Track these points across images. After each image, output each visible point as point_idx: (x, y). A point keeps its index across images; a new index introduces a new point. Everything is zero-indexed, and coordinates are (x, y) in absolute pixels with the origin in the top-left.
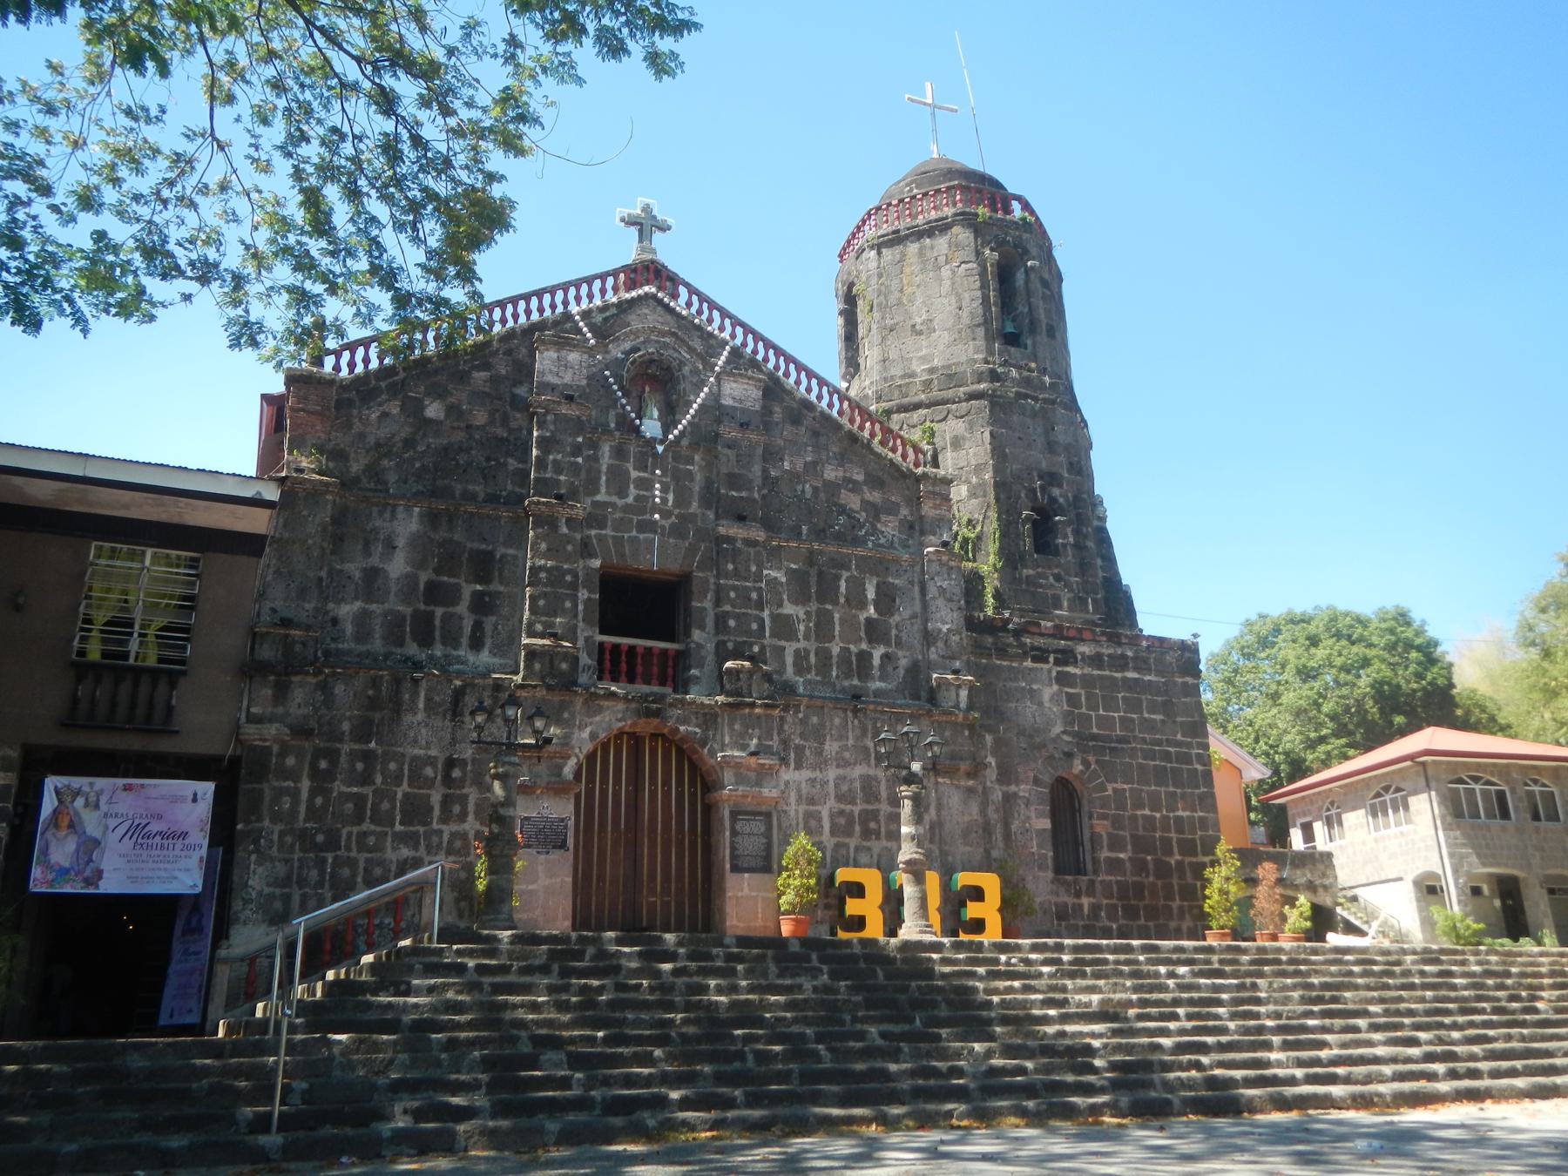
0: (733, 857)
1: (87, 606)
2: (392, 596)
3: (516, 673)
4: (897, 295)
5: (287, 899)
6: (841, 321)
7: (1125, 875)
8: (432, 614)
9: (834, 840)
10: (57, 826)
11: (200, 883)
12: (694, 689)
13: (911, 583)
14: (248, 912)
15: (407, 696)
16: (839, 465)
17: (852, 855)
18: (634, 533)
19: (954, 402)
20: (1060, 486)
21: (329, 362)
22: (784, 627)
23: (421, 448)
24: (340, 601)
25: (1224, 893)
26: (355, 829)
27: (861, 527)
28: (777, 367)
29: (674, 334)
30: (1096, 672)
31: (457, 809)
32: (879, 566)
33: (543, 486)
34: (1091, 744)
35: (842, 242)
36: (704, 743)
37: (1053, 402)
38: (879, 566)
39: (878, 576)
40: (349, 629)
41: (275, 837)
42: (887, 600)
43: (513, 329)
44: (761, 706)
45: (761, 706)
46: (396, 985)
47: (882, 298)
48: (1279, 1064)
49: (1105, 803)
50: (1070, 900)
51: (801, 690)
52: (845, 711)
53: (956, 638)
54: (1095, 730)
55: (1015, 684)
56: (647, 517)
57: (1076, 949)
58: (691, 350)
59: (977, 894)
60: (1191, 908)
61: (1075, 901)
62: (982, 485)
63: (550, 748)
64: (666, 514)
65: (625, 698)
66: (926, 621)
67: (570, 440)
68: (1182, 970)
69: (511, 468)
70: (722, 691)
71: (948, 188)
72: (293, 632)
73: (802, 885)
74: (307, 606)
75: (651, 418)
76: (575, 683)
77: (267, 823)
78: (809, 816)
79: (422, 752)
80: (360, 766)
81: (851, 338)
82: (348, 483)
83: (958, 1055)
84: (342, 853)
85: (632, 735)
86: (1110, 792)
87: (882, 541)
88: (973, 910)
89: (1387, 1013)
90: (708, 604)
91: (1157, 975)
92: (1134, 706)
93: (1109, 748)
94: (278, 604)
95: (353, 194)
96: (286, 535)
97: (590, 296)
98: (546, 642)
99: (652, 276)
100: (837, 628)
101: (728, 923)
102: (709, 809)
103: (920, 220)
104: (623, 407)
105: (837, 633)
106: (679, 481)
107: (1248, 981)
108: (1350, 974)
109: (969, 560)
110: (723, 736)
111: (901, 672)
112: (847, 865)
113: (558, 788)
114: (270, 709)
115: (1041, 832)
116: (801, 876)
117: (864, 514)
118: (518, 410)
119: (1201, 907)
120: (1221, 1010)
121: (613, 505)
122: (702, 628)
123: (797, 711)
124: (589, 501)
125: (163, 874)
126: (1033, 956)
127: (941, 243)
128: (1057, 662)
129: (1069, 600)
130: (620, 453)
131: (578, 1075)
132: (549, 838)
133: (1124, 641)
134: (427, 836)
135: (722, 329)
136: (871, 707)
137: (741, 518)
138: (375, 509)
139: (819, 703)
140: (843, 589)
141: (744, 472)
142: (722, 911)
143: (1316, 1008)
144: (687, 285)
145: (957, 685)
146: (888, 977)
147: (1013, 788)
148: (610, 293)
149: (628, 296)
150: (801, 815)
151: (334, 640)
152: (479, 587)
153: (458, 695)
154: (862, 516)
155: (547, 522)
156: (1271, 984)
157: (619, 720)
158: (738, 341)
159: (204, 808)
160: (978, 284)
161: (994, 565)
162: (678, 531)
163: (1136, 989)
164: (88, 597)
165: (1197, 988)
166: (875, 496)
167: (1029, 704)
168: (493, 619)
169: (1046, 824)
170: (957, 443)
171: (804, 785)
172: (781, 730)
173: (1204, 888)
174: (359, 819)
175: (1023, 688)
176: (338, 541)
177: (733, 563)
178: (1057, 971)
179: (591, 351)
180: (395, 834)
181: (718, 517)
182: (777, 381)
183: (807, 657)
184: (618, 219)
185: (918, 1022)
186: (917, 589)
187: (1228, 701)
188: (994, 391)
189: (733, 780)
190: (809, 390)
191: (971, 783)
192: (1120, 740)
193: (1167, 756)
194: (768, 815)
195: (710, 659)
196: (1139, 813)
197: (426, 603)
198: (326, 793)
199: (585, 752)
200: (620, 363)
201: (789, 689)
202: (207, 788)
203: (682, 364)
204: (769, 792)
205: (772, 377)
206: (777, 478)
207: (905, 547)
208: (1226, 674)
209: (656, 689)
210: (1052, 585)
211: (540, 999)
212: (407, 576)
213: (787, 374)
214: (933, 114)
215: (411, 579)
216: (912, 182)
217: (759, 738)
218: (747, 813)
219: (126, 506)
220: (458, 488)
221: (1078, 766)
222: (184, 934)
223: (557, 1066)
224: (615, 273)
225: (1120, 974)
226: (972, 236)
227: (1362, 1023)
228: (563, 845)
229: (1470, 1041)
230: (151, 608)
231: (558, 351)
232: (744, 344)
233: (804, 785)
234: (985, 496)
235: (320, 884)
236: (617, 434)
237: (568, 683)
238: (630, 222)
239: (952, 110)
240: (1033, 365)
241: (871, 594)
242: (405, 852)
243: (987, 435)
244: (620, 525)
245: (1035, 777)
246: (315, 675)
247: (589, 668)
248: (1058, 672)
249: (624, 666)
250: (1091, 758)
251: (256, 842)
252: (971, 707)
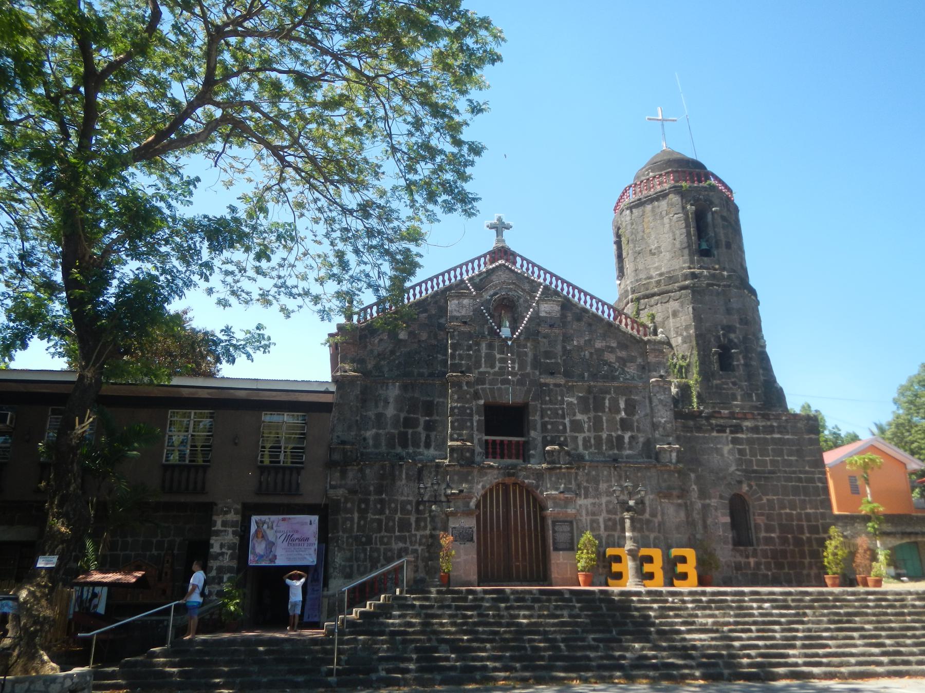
0: (554, 543)
1: (263, 440)
2: (389, 426)
3: (446, 458)
4: (641, 234)
5: (351, 567)
6: (615, 247)
7: (775, 545)
8: (407, 432)
9: (607, 533)
10: (257, 537)
11: (315, 560)
12: (532, 461)
13: (644, 398)
14: (335, 573)
15: (397, 473)
16: (603, 340)
17: (616, 541)
18: (499, 385)
19: (672, 292)
20: (735, 332)
21: (355, 318)
22: (577, 426)
23: (398, 354)
24: (367, 429)
25: (835, 554)
26: (378, 535)
27: (616, 372)
28: (568, 293)
29: (514, 284)
30: (755, 436)
31: (422, 524)
32: (626, 391)
33: (455, 367)
34: (753, 475)
35: (614, 205)
36: (537, 487)
37: (729, 286)
38: (626, 391)
39: (625, 395)
40: (371, 442)
41: (345, 540)
42: (631, 407)
43: (437, 291)
44: (565, 468)
45: (565, 468)
46: (386, 614)
47: (634, 236)
48: (794, 656)
49: (762, 507)
50: (743, 560)
51: (587, 457)
52: (610, 467)
53: (669, 425)
54: (755, 468)
55: (706, 446)
56: (505, 377)
57: (714, 594)
58: (523, 290)
59: (683, 560)
61: (746, 560)
62: (689, 336)
63: (464, 494)
64: (513, 374)
65: (498, 468)
66: (652, 417)
67: (466, 343)
68: (767, 605)
69: (439, 359)
70: (545, 461)
71: (666, 173)
72: (346, 447)
73: (588, 558)
74: (352, 433)
75: (505, 327)
76: (473, 462)
77: (341, 533)
78: (592, 521)
79: (405, 498)
80: (379, 506)
81: (620, 257)
82: (366, 374)
83: (627, 649)
84: (373, 546)
85: (503, 484)
86: (765, 501)
87: (628, 377)
88: (681, 568)
89: (876, 629)
90: (537, 418)
91: (752, 608)
92: (780, 453)
93: (764, 477)
94: (340, 434)
95: (357, 251)
96: (341, 402)
97: (473, 269)
98: (459, 443)
99: (503, 254)
100: (605, 425)
101: (553, 576)
102: (543, 519)
103: (652, 192)
104: (491, 323)
105: (605, 427)
106: (520, 358)
107: (801, 611)
108: (868, 607)
109: (682, 378)
111: (640, 445)
112: (614, 546)
113: (468, 513)
114: (339, 482)
115: (724, 524)
116: (588, 553)
117: (617, 364)
119: (823, 562)
120: (777, 627)
121: (489, 373)
122: (535, 430)
123: (584, 468)
124: (476, 372)
125: (300, 556)
126: (686, 598)
127: (664, 204)
128: (732, 432)
129: (741, 395)
130: (490, 346)
131: (453, 656)
132: (463, 537)
133: (772, 417)
134: (410, 538)
135: (539, 276)
136: (623, 464)
137: (552, 374)
138: (379, 386)
139: (596, 464)
140: (607, 404)
141: (552, 349)
142: (550, 569)
143: (832, 626)
144: (521, 256)
145: (670, 449)
146: (608, 610)
147: (708, 501)
148: (483, 266)
149: (491, 267)
150: (588, 522)
151: (365, 448)
152: (427, 418)
153: (420, 471)
154: (617, 365)
155: (457, 385)
156: (814, 613)
157: (495, 479)
158: (548, 282)
159: (315, 528)
160: (684, 225)
161: (696, 380)
162: (521, 383)
163: (736, 616)
164: (263, 437)
165: (771, 615)
166: (623, 354)
167: (715, 455)
168: (435, 433)
169: (728, 519)
170: (675, 314)
171: (589, 506)
172: (576, 479)
173: (823, 551)
174: (380, 531)
175: (712, 448)
176: (364, 401)
178: (696, 606)
179: (474, 298)
180: (396, 537)
181: (540, 374)
182: (568, 300)
183: (589, 441)
184: (485, 227)
185: (614, 633)
186: (647, 401)
187: (911, 414)
188: (694, 284)
189: (552, 505)
190: (585, 302)
191: (680, 501)
192: (771, 472)
193: (800, 480)
194: (571, 523)
195: (540, 445)
196: (782, 511)
197: (404, 427)
198: (365, 519)
200: (488, 301)
201: (581, 458)
202: (315, 518)
203: (519, 297)
204: (571, 511)
205: (566, 299)
206: (570, 350)
207: (641, 378)
208: (910, 398)
209: (514, 461)
210: (731, 388)
211: (444, 621)
212: (395, 415)
213: (574, 296)
214: (663, 125)
215: (396, 418)
216: (649, 168)
217: (565, 484)
218: (560, 522)
219: (275, 396)
220: (416, 371)
221: (745, 488)
222: (312, 581)
223: (446, 651)
224: (485, 256)
225: (731, 608)
226: (680, 199)
227: (855, 634)
228: (471, 540)
229: (916, 645)
230: (288, 440)
231: (458, 300)
232: (551, 283)
233: (589, 506)
234: (691, 342)
235: (365, 560)
236: (488, 337)
237: (470, 462)
238: (492, 227)
239: (673, 121)
240: (717, 266)
241: (622, 405)
242: (401, 545)
243: (691, 309)
244: (492, 382)
245: (720, 495)
246: (357, 465)
248: (732, 438)
249: (498, 451)
250: (753, 483)
251: (337, 542)
252: (678, 461)
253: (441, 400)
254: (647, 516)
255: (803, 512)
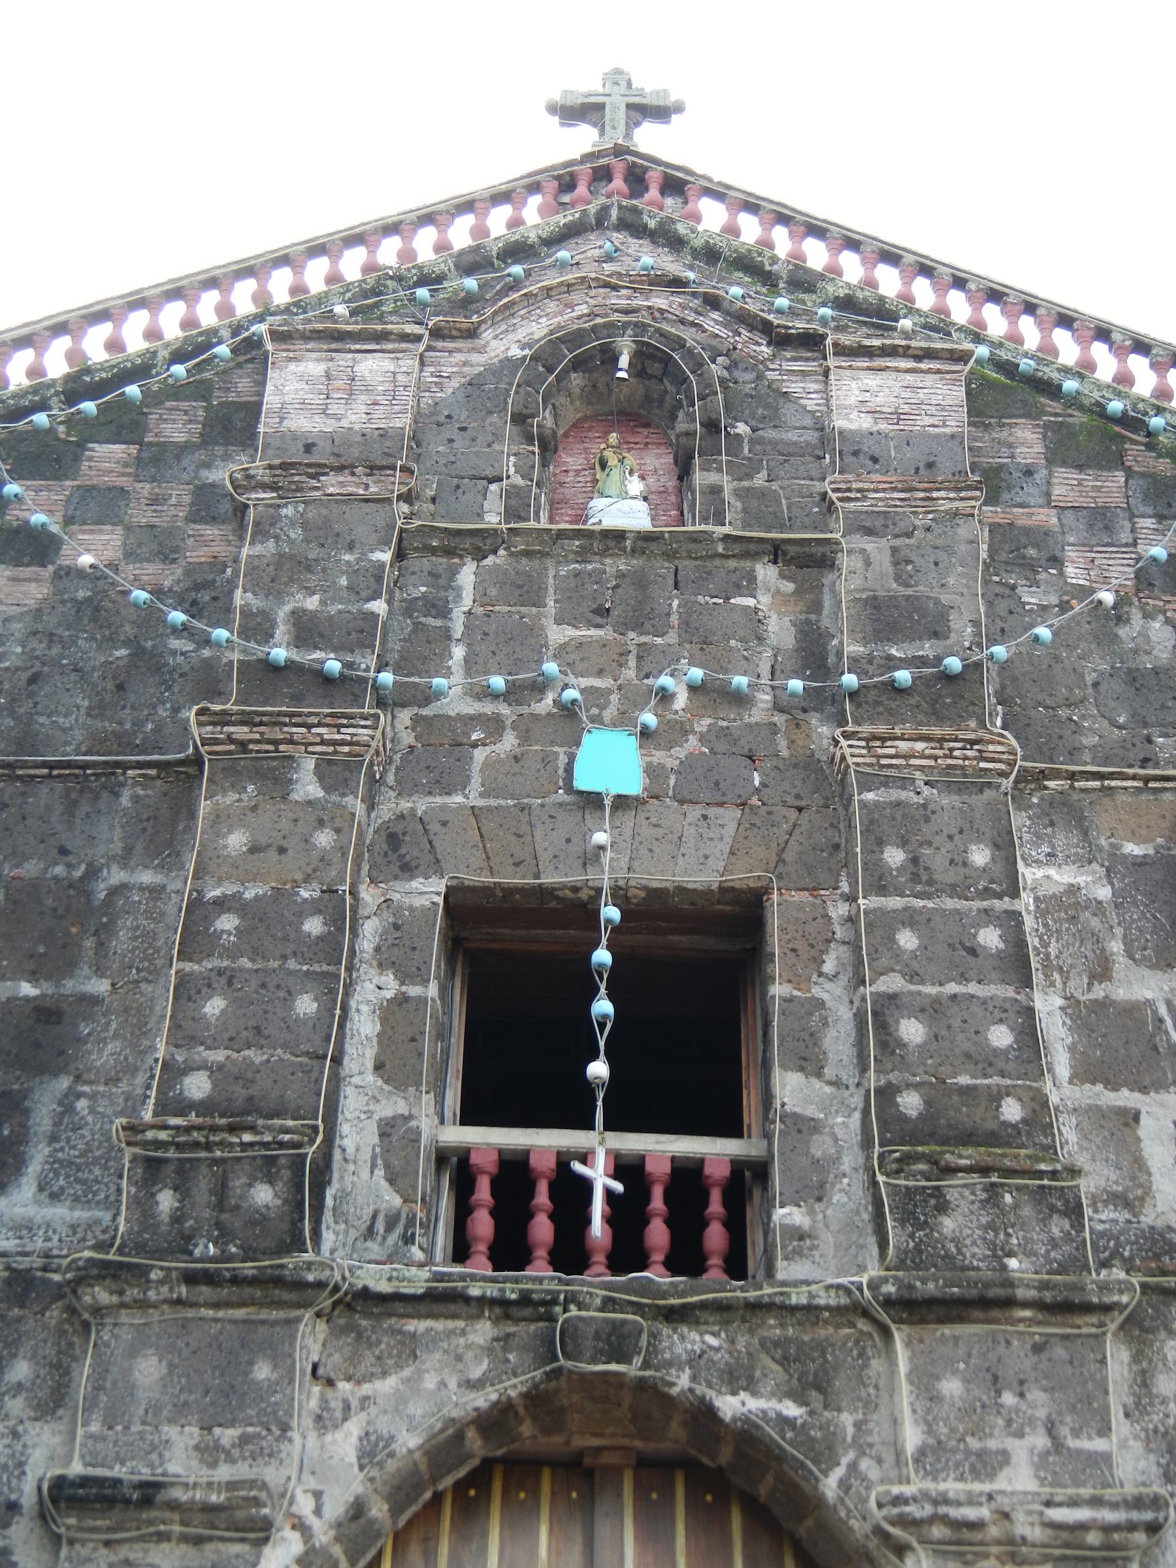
75: (624, 495)
110: (896, 1422)
118: (213, 520)
152: (27, 989)
177: (904, 843)
199: (335, 1508)
217: (1051, 1430)
247: (392, 1222)
249: (542, 1229)
253: (147, 877)
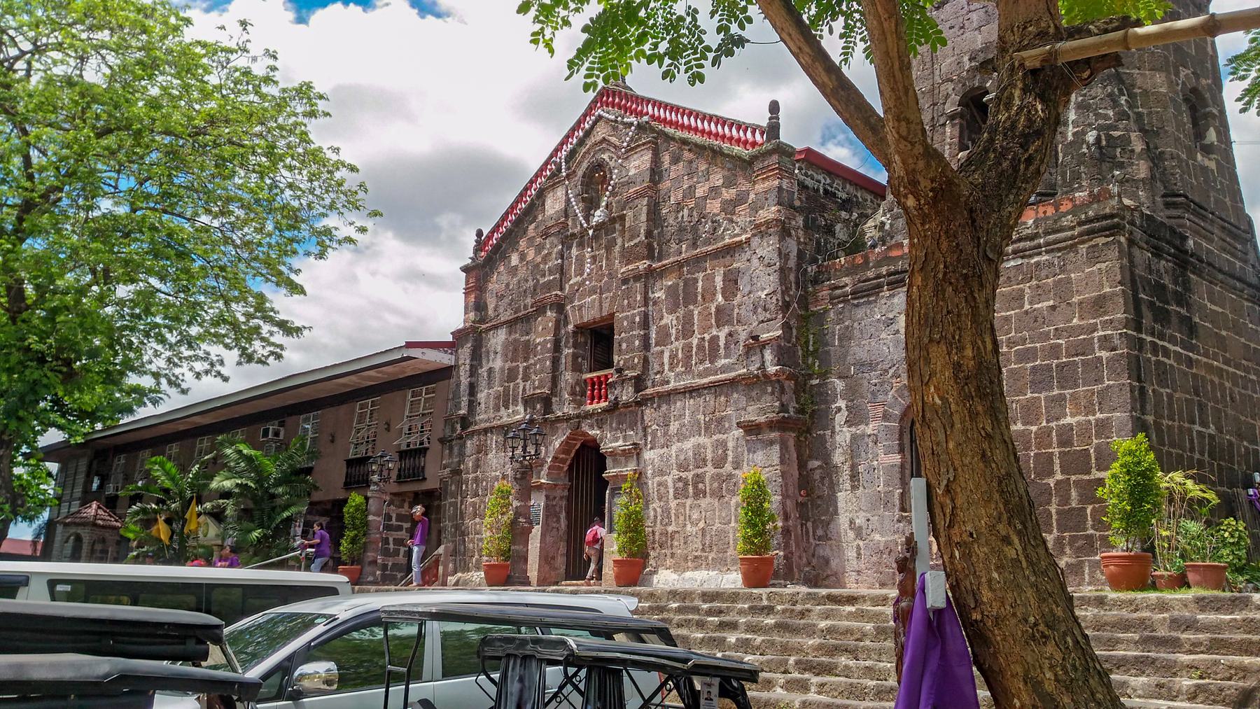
60: (1073, 540)
78: (660, 484)
140: (700, 290)
183: (676, 355)
193: (1055, 351)
241: (719, 282)
245: (885, 411)
254: (728, 467)
255: (1053, 424)
